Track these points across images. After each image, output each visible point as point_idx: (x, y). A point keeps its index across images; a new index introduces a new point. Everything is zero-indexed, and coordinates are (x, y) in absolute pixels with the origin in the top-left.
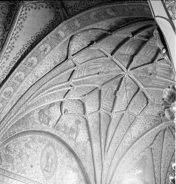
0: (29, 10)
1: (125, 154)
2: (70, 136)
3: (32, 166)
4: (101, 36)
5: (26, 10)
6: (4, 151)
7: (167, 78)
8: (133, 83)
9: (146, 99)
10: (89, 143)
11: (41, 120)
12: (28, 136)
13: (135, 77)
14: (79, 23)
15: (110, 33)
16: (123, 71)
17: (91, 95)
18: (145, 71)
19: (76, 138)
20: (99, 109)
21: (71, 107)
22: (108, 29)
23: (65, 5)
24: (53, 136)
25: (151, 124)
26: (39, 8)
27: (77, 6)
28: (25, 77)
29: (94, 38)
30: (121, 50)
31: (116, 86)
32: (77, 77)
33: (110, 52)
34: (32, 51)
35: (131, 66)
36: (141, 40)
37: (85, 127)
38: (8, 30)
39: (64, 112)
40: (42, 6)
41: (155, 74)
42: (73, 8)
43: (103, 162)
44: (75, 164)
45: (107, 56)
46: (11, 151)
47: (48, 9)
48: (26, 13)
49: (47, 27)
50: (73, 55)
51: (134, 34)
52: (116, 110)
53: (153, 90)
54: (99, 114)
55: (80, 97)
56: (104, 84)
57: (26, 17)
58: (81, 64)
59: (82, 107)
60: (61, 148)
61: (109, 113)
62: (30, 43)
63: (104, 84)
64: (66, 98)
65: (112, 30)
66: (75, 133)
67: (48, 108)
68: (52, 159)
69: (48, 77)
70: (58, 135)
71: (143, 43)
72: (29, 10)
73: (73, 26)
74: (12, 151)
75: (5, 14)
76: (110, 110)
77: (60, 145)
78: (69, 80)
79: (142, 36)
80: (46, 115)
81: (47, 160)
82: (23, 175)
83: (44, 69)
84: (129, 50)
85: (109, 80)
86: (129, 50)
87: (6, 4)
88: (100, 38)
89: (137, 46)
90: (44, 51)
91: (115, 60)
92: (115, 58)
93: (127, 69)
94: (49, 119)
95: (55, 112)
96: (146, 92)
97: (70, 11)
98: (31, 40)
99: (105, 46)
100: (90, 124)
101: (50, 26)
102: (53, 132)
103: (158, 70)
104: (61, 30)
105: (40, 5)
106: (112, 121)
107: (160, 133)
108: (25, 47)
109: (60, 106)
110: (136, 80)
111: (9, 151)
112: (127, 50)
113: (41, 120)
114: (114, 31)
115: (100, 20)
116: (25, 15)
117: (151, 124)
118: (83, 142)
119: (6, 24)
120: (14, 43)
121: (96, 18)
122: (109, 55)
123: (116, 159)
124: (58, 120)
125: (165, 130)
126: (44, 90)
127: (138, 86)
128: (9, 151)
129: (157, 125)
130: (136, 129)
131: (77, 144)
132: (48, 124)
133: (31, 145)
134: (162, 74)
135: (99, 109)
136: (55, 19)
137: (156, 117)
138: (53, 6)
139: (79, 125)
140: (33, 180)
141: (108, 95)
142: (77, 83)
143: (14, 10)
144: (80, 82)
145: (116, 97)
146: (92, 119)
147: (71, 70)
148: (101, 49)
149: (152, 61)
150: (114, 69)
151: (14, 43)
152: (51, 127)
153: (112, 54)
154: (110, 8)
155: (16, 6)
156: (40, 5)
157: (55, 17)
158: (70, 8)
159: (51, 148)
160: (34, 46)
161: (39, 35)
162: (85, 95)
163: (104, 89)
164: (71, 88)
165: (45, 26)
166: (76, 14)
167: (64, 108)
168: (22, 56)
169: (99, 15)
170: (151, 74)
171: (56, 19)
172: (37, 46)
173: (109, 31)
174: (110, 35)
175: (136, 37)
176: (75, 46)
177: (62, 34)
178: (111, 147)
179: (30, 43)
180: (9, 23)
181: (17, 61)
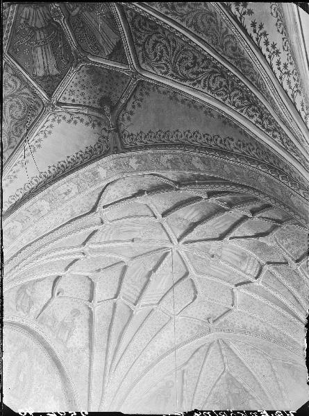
0: (59, 121)
1: (143, 376)
2: (59, 335)
4: (159, 185)
5: (54, 120)
7: (235, 267)
8: (181, 263)
9: (193, 291)
10: (87, 350)
11: (19, 303)
13: (187, 255)
14: (136, 163)
15: (177, 187)
16: (171, 242)
17: (109, 271)
18: (206, 250)
20: (116, 297)
21: (72, 287)
22: (176, 180)
23: (122, 129)
24: (31, 332)
25: (192, 332)
26: (75, 122)
27: (141, 137)
28: (22, 232)
29: (145, 187)
30: (180, 212)
31: (154, 264)
32: (97, 240)
33: (162, 211)
34: (46, 191)
35: (186, 238)
36: (217, 206)
37: (86, 323)
38: (13, 147)
39: (58, 294)
40: (82, 121)
41: (220, 257)
42: (135, 137)
43: (106, 385)
44: (59, 385)
45: (155, 216)
47: (90, 127)
48: (51, 126)
49: (81, 155)
50: (104, 207)
51: (210, 194)
52: (143, 301)
53: (207, 280)
54: (115, 305)
55: (92, 272)
56: (134, 258)
57: (50, 132)
58: (110, 221)
59: (89, 288)
61: (132, 306)
62: (45, 176)
63: (134, 258)
64: (69, 272)
65: (181, 183)
66: (68, 332)
67: (34, 285)
68: (25, 375)
69: (57, 234)
70: (40, 333)
71: (219, 210)
72: (59, 121)
73: (124, 165)
75: (14, 118)
76: (134, 302)
77: (40, 349)
78: (84, 244)
79: (221, 201)
80: (28, 296)
81: (18, 376)
83: (53, 221)
84: (192, 214)
85: (145, 252)
86: (192, 214)
87: (20, 101)
88: (154, 190)
89: (206, 211)
90: (66, 194)
91: (165, 225)
92: (167, 222)
93: (179, 240)
94: (31, 303)
95: (44, 292)
96: (196, 281)
97: (128, 140)
98: (47, 172)
99: (159, 202)
100: (96, 319)
101: (86, 156)
102: (33, 326)
103: (224, 252)
104: (103, 168)
105: (78, 118)
106: (134, 319)
107: (203, 348)
108: (33, 181)
109: (52, 283)
110: (186, 259)
112: (189, 214)
113: (19, 303)
114: (185, 185)
115: (174, 169)
116: (49, 129)
117: (192, 332)
119: (12, 136)
120: (18, 171)
121: (169, 164)
122: (159, 215)
123: (126, 383)
124: (45, 307)
125: (211, 344)
126: (42, 255)
127: (187, 270)
129: (202, 335)
130: (166, 339)
131: (68, 351)
132: (28, 312)
134: (229, 260)
135: (116, 297)
136: (96, 147)
137: (203, 322)
138: (99, 124)
141: (136, 276)
142: (92, 251)
143: (33, 115)
144: (104, 249)
145: (148, 281)
146: (100, 310)
147: (92, 229)
148: (152, 206)
149: (221, 237)
150: (158, 237)
151: (18, 171)
153: (164, 215)
154: (199, 157)
155: (37, 110)
156: (78, 118)
157: (97, 143)
158: (129, 136)
159: (25, 355)
160: (50, 184)
161: (62, 166)
162: (99, 270)
163: (132, 265)
164: (83, 256)
165: (77, 154)
166: (136, 148)
167: (60, 285)
168: (25, 194)
169: (177, 162)
170: (213, 256)
171: (99, 147)
172: (56, 184)
173: (176, 183)
174: (177, 190)
175: (213, 200)
176: (112, 194)
177: (102, 172)
178: (122, 362)
179: (45, 176)
180: (18, 136)
181: (14, 202)
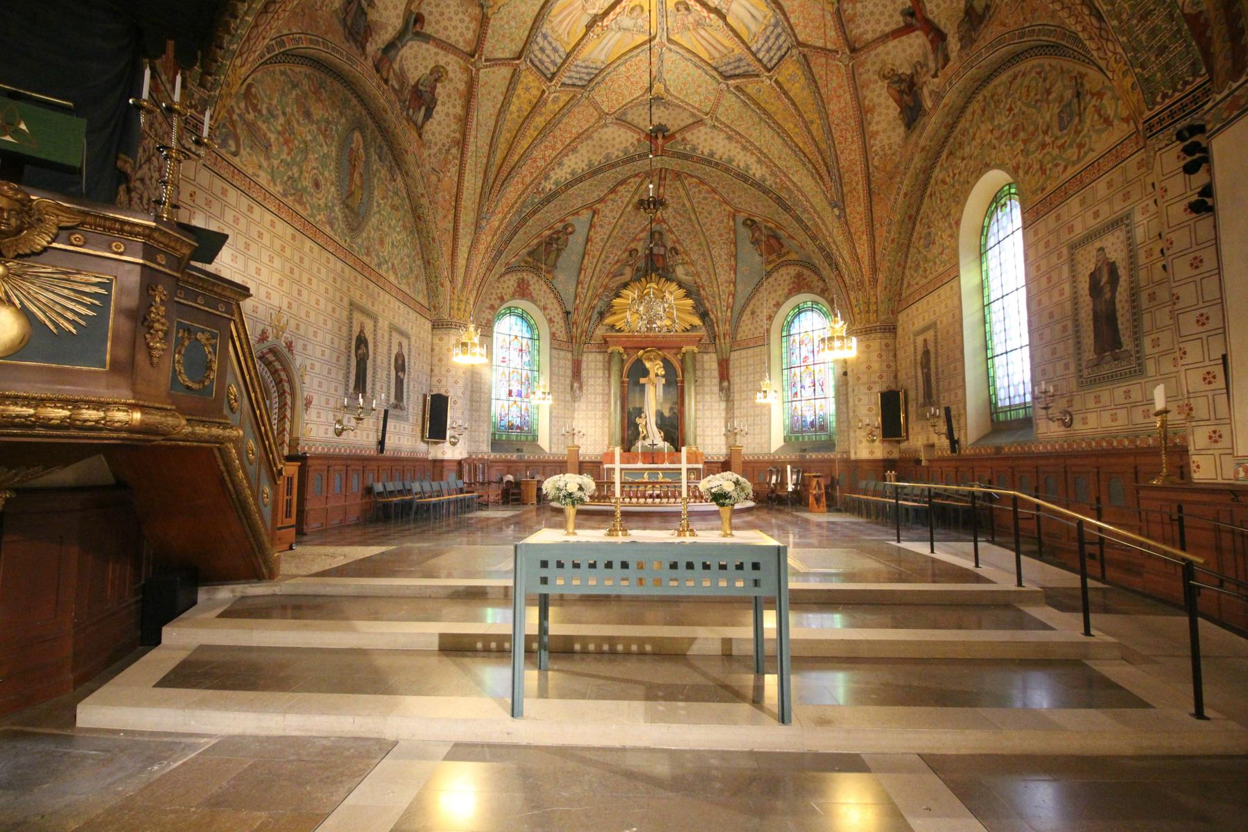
2: (411, 111)
3: (317, 185)
6: (242, 105)
12: (303, 69)
19: (422, 127)
46: (260, 112)
60: (381, 147)
66: (423, 109)
68: (361, 175)
74: (264, 111)
81: (352, 175)
82: (298, 208)
111: (255, 109)
118: (440, 144)
128: (255, 109)
133: (312, 110)
139: (439, 85)
140: (322, 228)
152: (370, 63)
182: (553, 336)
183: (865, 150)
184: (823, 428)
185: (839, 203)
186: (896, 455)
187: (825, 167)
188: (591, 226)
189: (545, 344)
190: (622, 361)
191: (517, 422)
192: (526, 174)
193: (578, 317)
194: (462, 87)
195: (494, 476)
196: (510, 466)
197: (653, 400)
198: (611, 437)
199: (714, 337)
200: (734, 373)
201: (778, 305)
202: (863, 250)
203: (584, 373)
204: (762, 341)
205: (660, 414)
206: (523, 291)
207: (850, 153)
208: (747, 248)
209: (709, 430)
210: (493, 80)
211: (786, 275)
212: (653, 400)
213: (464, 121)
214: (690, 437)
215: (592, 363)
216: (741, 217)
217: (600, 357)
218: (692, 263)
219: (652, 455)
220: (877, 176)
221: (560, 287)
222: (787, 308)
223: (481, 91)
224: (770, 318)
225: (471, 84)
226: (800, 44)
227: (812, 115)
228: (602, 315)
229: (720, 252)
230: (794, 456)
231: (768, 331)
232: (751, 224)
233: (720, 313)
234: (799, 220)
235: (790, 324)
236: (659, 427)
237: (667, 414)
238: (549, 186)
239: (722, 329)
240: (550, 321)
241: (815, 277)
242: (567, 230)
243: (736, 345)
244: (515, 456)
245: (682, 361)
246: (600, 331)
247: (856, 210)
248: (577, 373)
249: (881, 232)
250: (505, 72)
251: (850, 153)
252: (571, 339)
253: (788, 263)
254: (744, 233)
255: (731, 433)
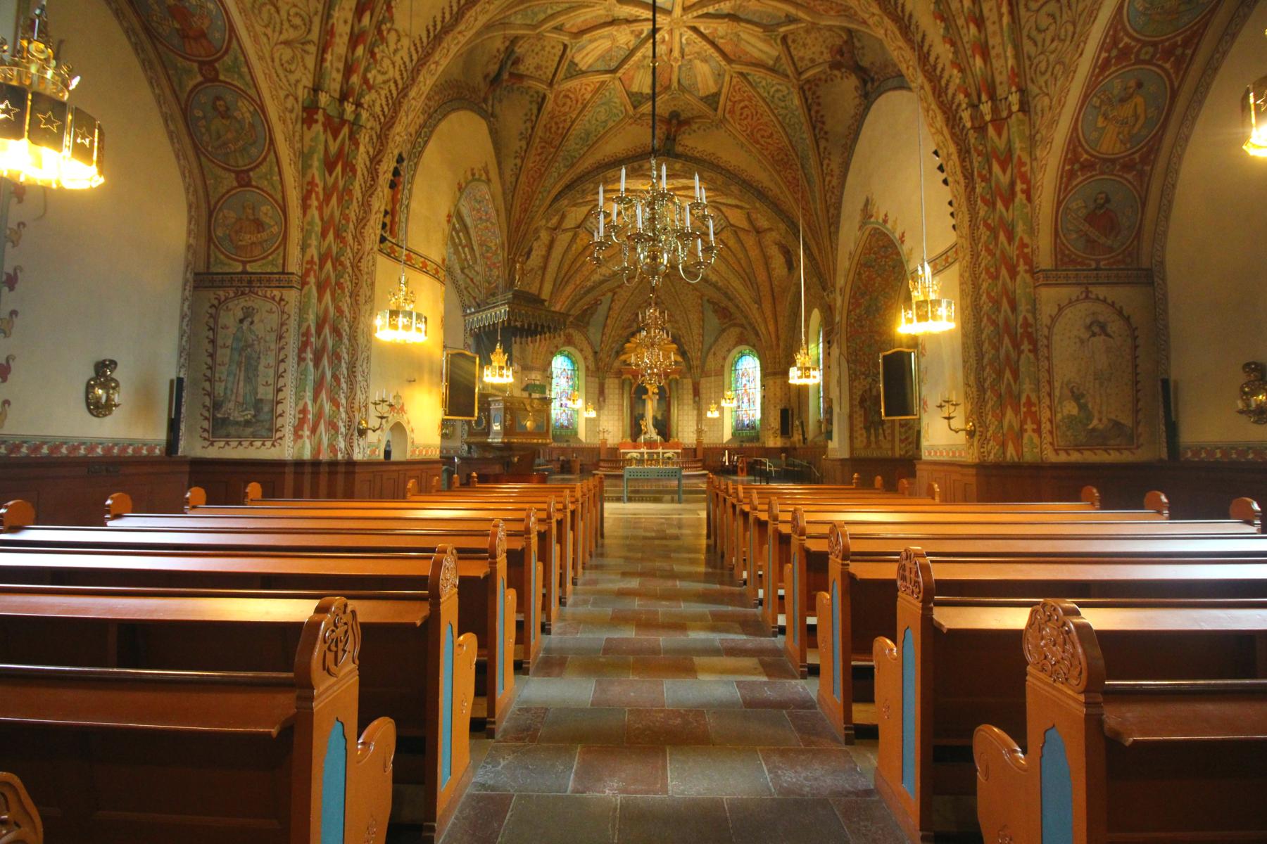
182: (587, 368)
183: (770, 277)
184: (753, 428)
185: (759, 301)
186: (788, 445)
187: (749, 279)
188: (613, 301)
189: (582, 374)
190: (631, 385)
191: (566, 423)
192: (578, 279)
193: (603, 355)
194: (547, 242)
195: (555, 457)
196: (563, 451)
197: (651, 409)
198: (624, 432)
199: (690, 368)
200: (703, 391)
201: (729, 351)
202: (772, 328)
203: (606, 391)
204: (720, 373)
205: (655, 418)
206: (569, 341)
207: (762, 276)
208: (710, 314)
209: (686, 432)
210: (563, 239)
211: (735, 331)
212: (651, 409)
213: (547, 258)
214: (674, 433)
215: (612, 385)
216: (706, 298)
217: (616, 381)
218: (676, 322)
219: (650, 444)
220: (776, 290)
221: (591, 336)
222: (735, 352)
223: (557, 243)
224: (724, 359)
225: (552, 242)
226: (732, 225)
227: (741, 255)
228: (618, 354)
229: (694, 317)
230: (736, 445)
231: (723, 366)
232: (714, 304)
233: (694, 354)
234: (737, 307)
235: (736, 362)
236: (655, 426)
237: (659, 418)
238: (589, 284)
239: (696, 363)
240: (585, 358)
241: (750, 339)
242: (597, 303)
243: (705, 374)
244: (565, 445)
245: (669, 385)
246: (617, 364)
247: (767, 306)
248: (602, 392)
249: (780, 319)
250: (570, 234)
251: (762, 276)
252: (598, 369)
253: (735, 325)
254: (707, 305)
255: (699, 432)
